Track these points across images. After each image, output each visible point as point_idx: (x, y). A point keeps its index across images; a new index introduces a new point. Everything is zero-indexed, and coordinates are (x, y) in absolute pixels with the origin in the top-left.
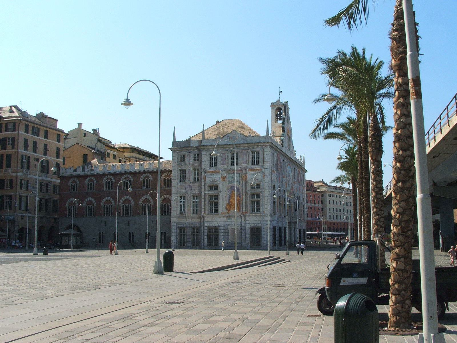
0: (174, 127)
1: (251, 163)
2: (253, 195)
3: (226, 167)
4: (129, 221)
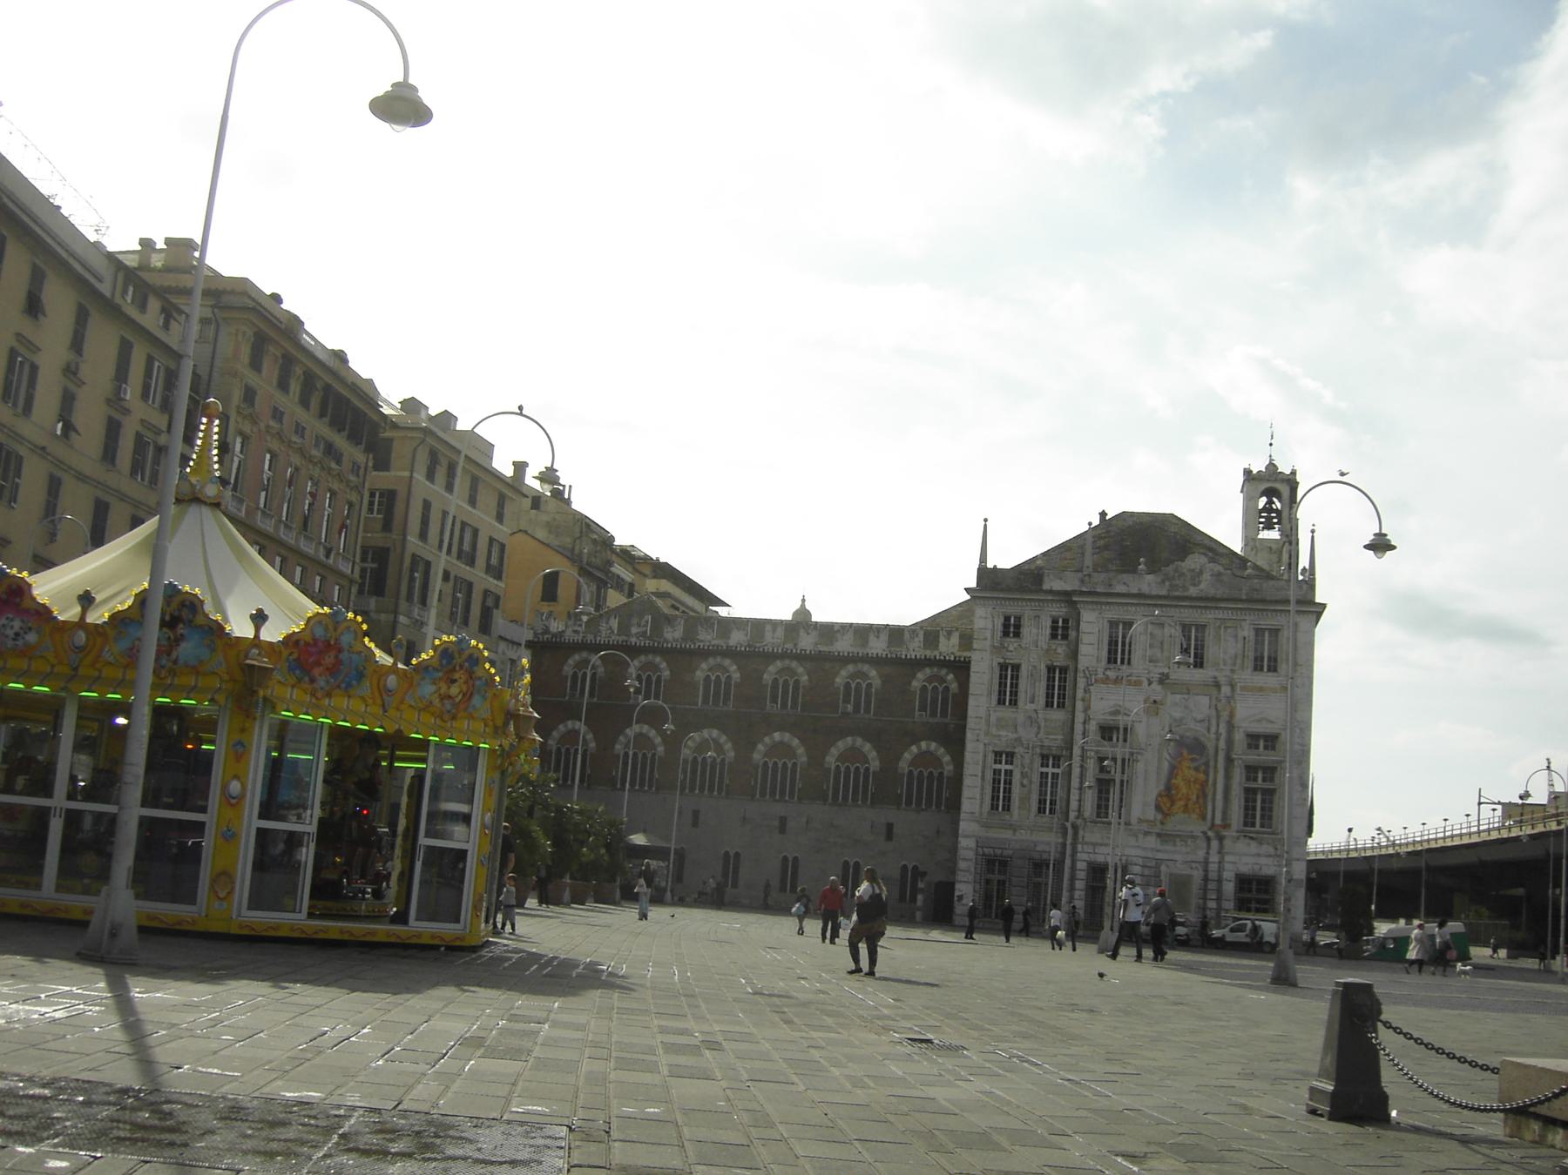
0: (986, 520)
1: (1250, 664)
2: (1251, 770)
3: (1166, 671)
4: (783, 821)
